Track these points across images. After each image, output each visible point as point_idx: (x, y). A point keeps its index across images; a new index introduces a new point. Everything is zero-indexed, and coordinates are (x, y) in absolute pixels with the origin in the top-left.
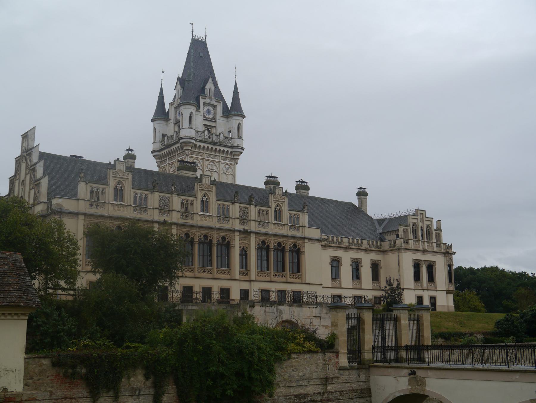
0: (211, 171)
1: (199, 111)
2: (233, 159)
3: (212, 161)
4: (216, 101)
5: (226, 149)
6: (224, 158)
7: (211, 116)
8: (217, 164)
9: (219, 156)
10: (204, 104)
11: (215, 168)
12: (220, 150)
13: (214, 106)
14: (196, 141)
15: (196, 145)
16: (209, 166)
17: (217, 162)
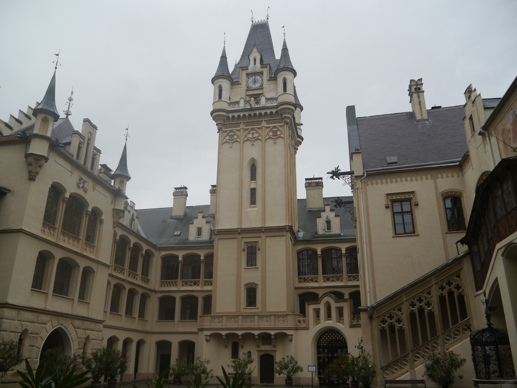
0: (251, 140)
1: (240, 84)
2: (283, 119)
3: (253, 129)
4: (262, 68)
5: (268, 111)
6: (268, 122)
7: (258, 85)
8: (259, 131)
9: (262, 121)
10: (248, 75)
11: (256, 135)
12: (260, 114)
13: (261, 74)
14: (228, 112)
15: (228, 117)
16: (250, 136)
17: (259, 128)
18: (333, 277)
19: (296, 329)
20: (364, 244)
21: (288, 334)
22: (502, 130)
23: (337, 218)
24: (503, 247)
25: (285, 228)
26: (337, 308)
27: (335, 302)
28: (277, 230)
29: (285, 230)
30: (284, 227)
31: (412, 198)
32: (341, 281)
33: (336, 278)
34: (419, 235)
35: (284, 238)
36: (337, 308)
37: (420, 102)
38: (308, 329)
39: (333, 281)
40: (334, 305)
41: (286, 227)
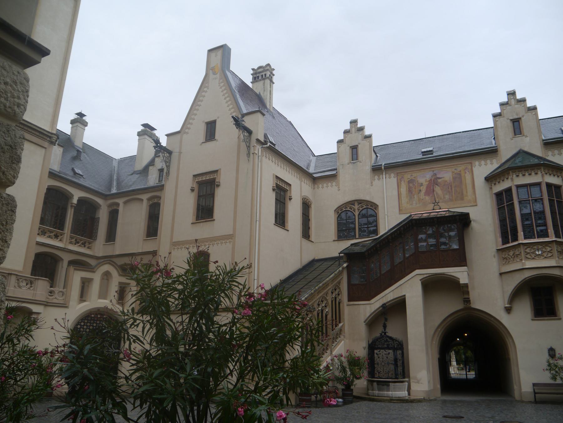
18: (51, 232)
19: (46, 304)
20: (256, 222)
21: (34, 311)
22: (409, 179)
23: (60, 149)
25: (50, 137)
26: (120, 283)
27: (120, 275)
28: (38, 134)
29: (48, 139)
30: (50, 135)
31: (288, 190)
32: (60, 240)
33: (54, 235)
34: (288, 231)
35: (44, 150)
36: (120, 283)
37: (270, 91)
38: (67, 307)
39: (49, 237)
40: (117, 279)
41: (53, 136)
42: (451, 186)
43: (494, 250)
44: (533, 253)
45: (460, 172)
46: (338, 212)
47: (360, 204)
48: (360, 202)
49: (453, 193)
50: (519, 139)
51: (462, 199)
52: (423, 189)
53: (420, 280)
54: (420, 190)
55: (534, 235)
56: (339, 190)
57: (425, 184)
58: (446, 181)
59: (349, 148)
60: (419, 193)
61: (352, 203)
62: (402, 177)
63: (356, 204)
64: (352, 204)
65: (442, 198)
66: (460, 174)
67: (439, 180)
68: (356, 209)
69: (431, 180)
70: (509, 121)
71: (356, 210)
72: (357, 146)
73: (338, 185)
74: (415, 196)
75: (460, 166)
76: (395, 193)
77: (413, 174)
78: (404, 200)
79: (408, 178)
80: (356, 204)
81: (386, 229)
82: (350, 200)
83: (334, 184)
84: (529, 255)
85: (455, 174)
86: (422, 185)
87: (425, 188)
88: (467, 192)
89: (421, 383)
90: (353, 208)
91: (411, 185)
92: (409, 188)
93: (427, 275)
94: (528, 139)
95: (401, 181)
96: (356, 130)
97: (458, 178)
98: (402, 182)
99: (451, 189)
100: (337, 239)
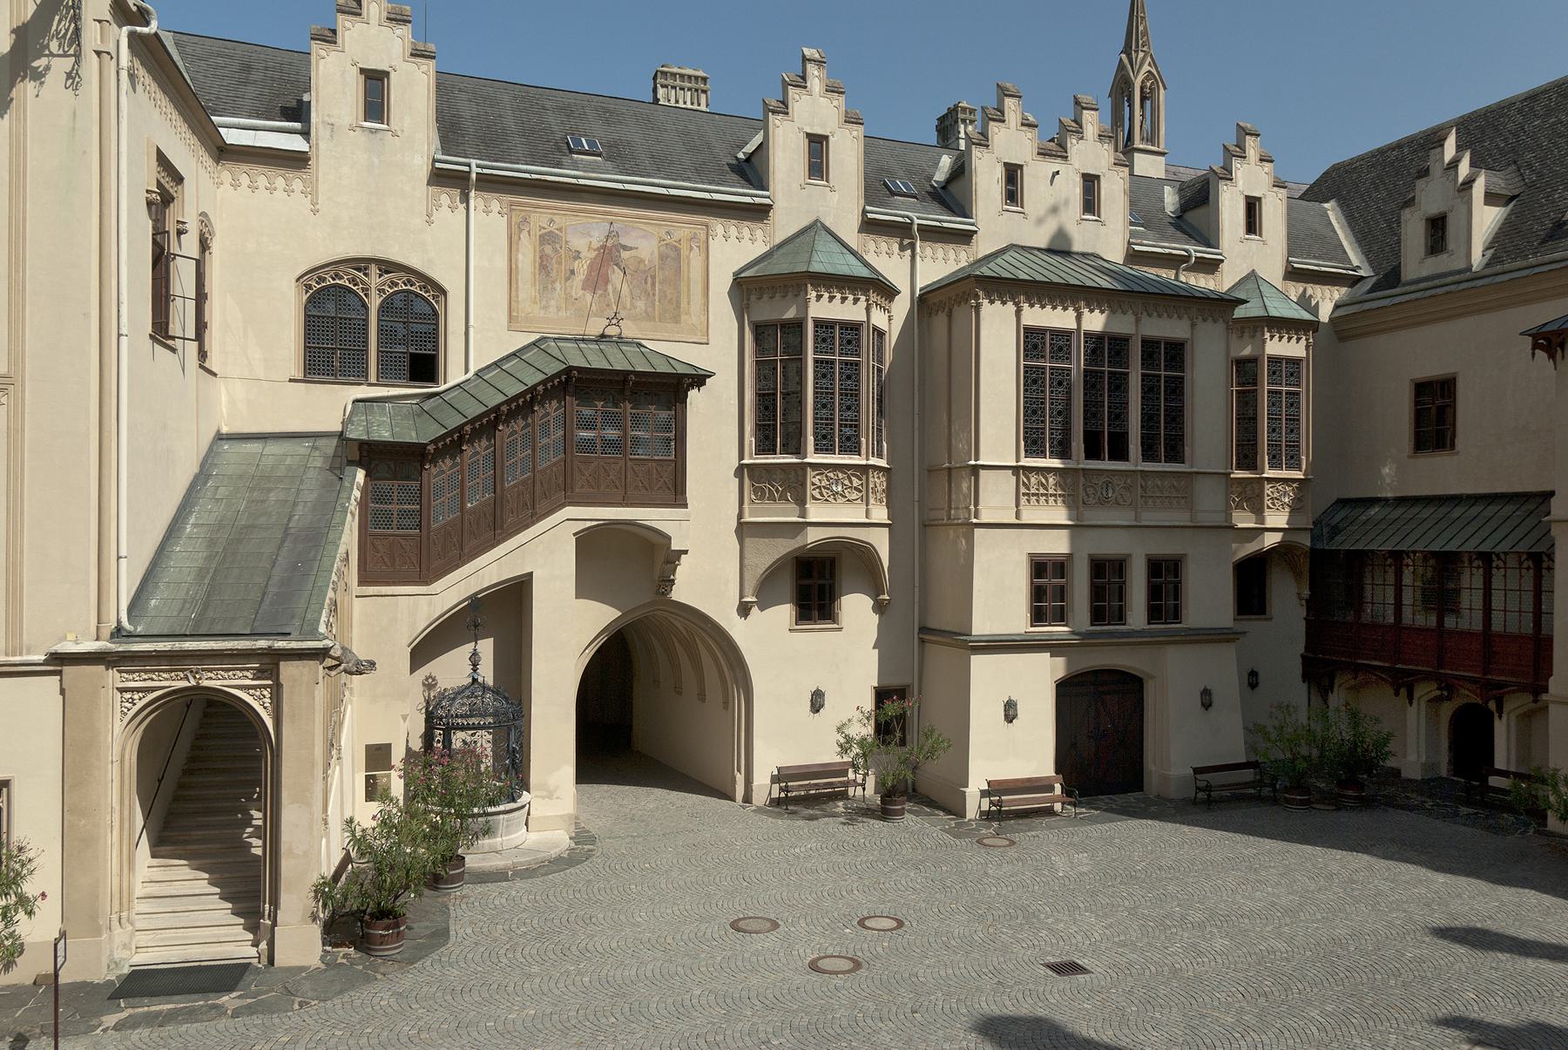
22: (543, 231)
24: (600, 520)
42: (653, 278)
43: (734, 463)
44: (828, 489)
45: (677, 244)
46: (309, 287)
47: (387, 272)
48: (387, 266)
49: (657, 298)
50: (818, 187)
51: (676, 319)
52: (582, 268)
53: (574, 535)
54: (572, 272)
55: (833, 445)
56: (315, 212)
57: (588, 256)
58: (641, 261)
59: (355, 71)
60: (567, 279)
61: (361, 264)
62: (525, 220)
63: (374, 270)
64: (359, 270)
65: (628, 306)
66: (677, 250)
67: (625, 254)
68: (373, 286)
69: (604, 247)
70: (802, 135)
71: (374, 293)
72: (387, 74)
73: (311, 192)
74: (558, 286)
75: (683, 226)
76: (502, 263)
77: (557, 218)
78: (526, 290)
79: (542, 228)
80: (374, 270)
81: (467, 371)
82: (353, 254)
83: (297, 185)
84: (818, 490)
85: (666, 244)
86: (577, 255)
87: (585, 267)
88: (689, 303)
89: (557, 798)
90: (363, 282)
91: (548, 249)
92: (541, 258)
93: (595, 523)
94: (836, 196)
95: (520, 231)
96: (385, 14)
97: (672, 256)
98: (524, 235)
99: (653, 284)
100: (301, 376)
